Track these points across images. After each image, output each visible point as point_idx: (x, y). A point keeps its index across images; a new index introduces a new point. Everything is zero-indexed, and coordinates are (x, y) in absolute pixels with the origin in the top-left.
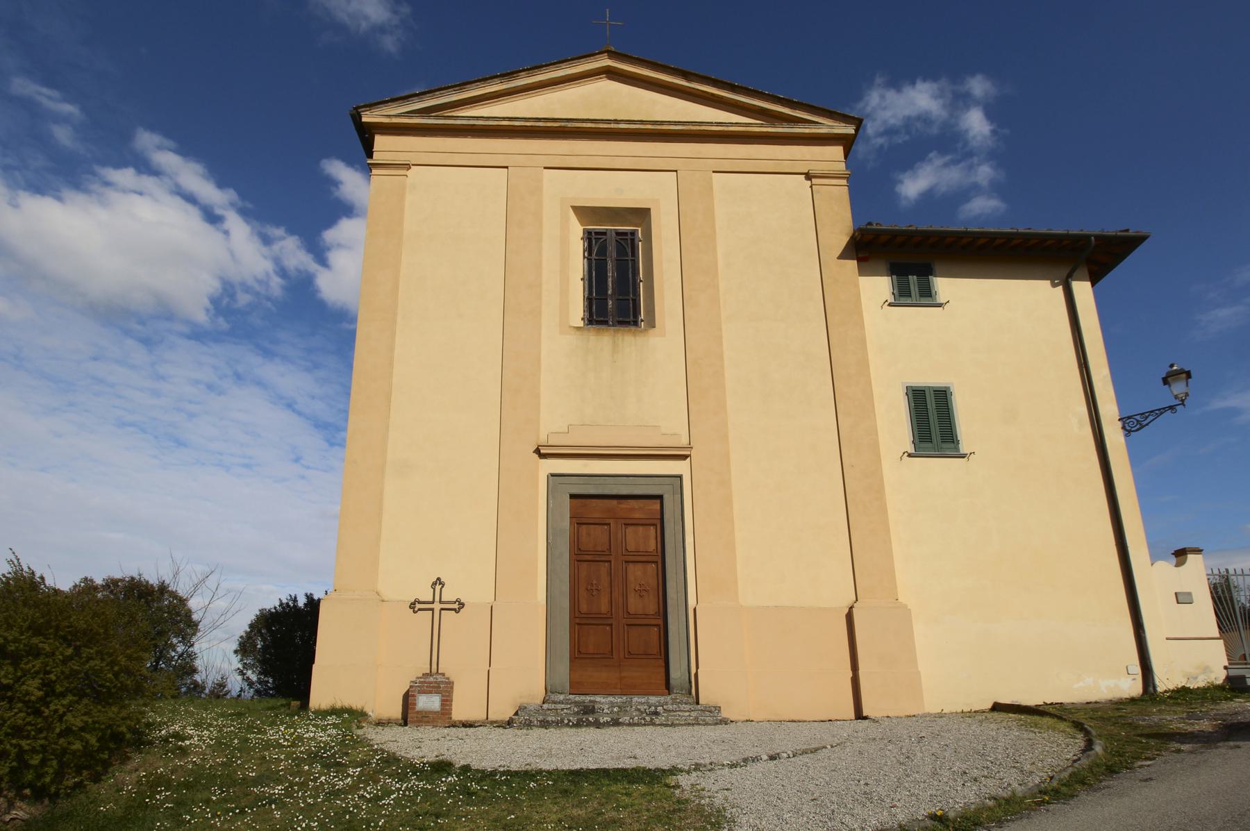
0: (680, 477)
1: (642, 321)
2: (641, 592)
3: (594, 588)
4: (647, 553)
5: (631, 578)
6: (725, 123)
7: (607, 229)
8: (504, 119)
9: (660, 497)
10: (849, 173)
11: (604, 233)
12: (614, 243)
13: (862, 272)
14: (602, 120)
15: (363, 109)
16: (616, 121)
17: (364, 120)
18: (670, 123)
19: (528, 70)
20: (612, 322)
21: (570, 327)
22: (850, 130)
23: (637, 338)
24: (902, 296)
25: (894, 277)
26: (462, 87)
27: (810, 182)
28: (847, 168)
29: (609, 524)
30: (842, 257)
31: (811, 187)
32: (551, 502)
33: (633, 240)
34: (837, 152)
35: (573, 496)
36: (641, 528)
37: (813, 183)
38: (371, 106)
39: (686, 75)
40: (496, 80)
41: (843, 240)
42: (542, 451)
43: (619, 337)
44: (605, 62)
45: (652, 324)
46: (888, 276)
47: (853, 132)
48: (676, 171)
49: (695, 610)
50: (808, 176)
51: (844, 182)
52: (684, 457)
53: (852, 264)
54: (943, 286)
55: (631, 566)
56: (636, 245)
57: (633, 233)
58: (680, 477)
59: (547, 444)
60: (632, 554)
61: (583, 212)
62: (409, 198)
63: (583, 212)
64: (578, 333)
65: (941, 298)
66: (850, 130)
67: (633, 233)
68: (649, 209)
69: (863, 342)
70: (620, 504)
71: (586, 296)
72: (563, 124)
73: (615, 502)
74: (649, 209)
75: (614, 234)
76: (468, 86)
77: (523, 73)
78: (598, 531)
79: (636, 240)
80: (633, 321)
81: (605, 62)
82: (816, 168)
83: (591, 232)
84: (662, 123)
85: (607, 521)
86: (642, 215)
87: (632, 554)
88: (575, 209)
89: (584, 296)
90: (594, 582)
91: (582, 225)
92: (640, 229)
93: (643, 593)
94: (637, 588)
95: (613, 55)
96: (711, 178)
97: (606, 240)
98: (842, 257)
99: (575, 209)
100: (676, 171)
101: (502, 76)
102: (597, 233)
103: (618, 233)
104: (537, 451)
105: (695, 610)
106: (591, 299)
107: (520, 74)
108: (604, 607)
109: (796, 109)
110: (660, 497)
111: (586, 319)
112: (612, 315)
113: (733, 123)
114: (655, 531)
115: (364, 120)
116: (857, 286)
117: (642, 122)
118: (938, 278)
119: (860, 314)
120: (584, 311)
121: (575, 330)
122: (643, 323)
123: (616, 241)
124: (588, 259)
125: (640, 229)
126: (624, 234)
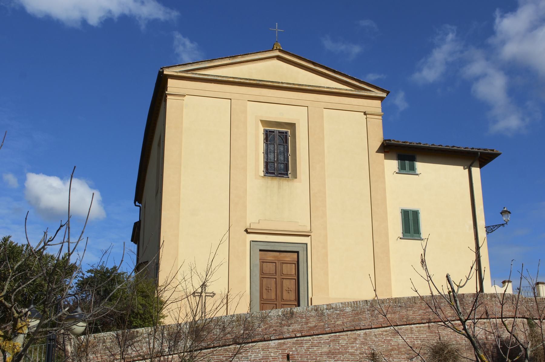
0: (306, 244)
1: (290, 174)
2: (288, 291)
3: (269, 289)
4: (291, 275)
5: (284, 285)
6: (330, 88)
7: (275, 130)
8: (231, 78)
9: (298, 252)
10: (383, 114)
11: (273, 132)
12: (278, 137)
13: (386, 158)
14: (276, 82)
15: (165, 68)
16: (282, 83)
17: (165, 73)
18: (306, 85)
19: (242, 55)
20: (277, 173)
21: (260, 176)
22: (384, 95)
23: (289, 182)
24: (402, 169)
25: (399, 161)
26: (211, 61)
27: (366, 116)
28: (382, 111)
29: (275, 263)
30: (378, 152)
31: (366, 118)
32: (252, 252)
33: (286, 136)
34: (378, 103)
35: (261, 250)
36: (289, 265)
37: (367, 117)
38: (168, 67)
39: (314, 64)
40: (227, 58)
41: (379, 144)
42: (249, 231)
43: (281, 181)
44: (277, 53)
45: (295, 177)
46: (397, 160)
47: (385, 96)
48: (307, 107)
49: (311, 299)
50: (365, 114)
51: (380, 117)
52: (308, 236)
53: (382, 155)
54: (420, 166)
55: (284, 281)
56: (288, 139)
57: (286, 133)
58: (306, 244)
59: (249, 228)
60: (285, 275)
61: (265, 123)
62: (184, 110)
63: (265, 123)
64: (263, 179)
65: (418, 172)
66: (384, 95)
67: (286, 133)
68: (295, 124)
69: (384, 190)
70: (280, 254)
71: (265, 161)
72: (258, 82)
73: (278, 253)
74: (295, 124)
75: (278, 132)
76: (214, 61)
77: (240, 56)
78: (272, 266)
79: (288, 136)
80: (286, 174)
81: (277, 53)
82: (368, 110)
83: (267, 131)
84: (303, 85)
85: (276, 261)
86: (292, 126)
87: (285, 275)
88: (262, 121)
89: (264, 161)
90: (269, 286)
91: (263, 127)
92: (289, 131)
93: (290, 291)
94: (287, 289)
95: (280, 51)
96: (323, 111)
97: (274, 135)
98: (378, 152)
99: (262, 121)
100: (307, 107)
101: (230, 57)
102: (270, 131)
103: (280, 132)
104: (246, 231)
105: (311, 299)
106: (267, 162)
107: (238, 57)
108: (273, 297)
109: (361, 84)
110: (298, 252)
111: (265, 171)
112: (277, 170)
113: (334, 88)
114: (294, 265)
115: (165, 73)
116: (383, 164)
117: (294, 84)
118: (417, 163)
119: (384, 178)
120: (264, 168)
121: (262, 177)
122: (290, 174)
123: (279, 135)
124: (266, 143)
125: (289, 131)
126: (283, 133)
